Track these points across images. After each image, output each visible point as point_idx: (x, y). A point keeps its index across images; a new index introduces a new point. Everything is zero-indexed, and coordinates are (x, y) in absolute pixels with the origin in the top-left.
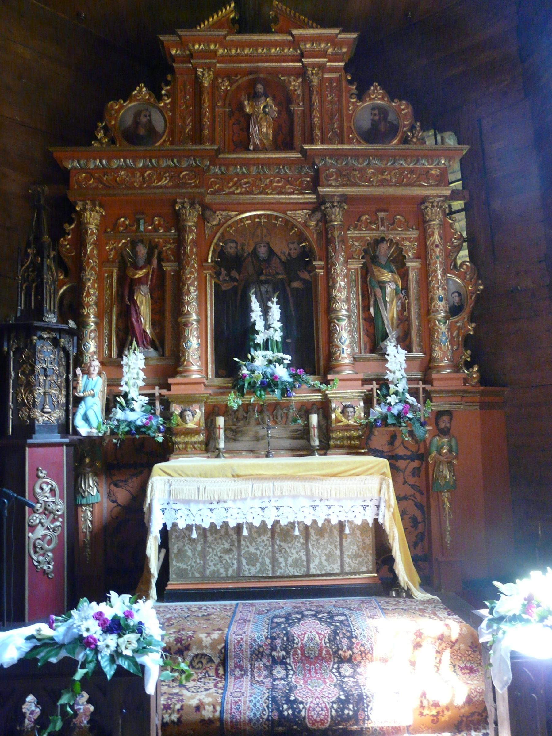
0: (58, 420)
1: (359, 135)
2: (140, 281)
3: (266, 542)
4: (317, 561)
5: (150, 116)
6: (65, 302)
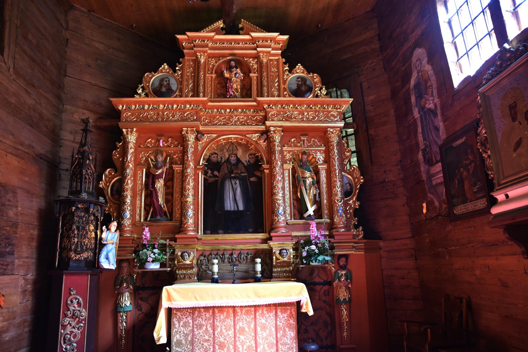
1: (290, 92)
2: (160, 176)
3: (231, 335)
4: (262, 347)
5: (169, 81)
6: (114, 188)
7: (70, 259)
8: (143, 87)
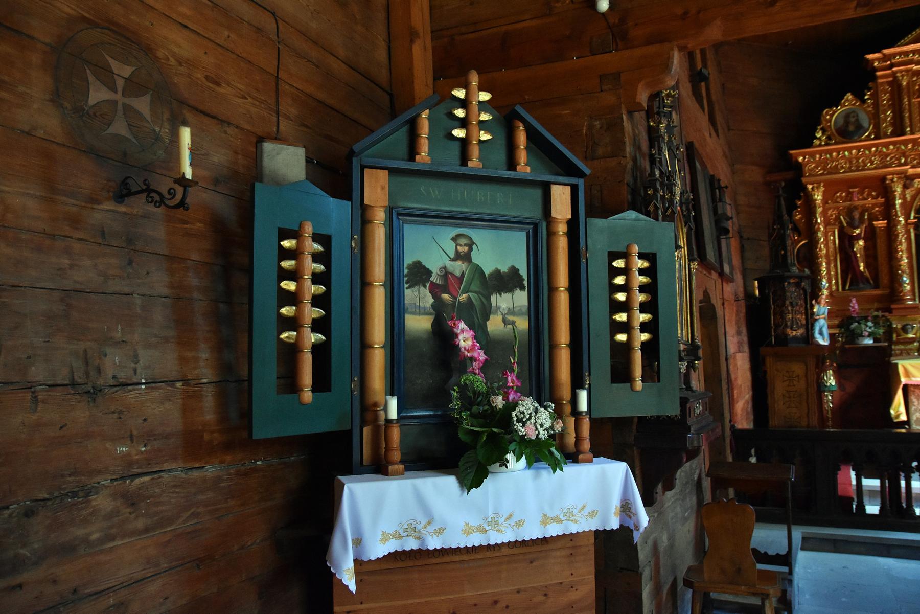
0: (802, 335)
2: (858, 237)
7: (787, 335)
8: (822, 129)
